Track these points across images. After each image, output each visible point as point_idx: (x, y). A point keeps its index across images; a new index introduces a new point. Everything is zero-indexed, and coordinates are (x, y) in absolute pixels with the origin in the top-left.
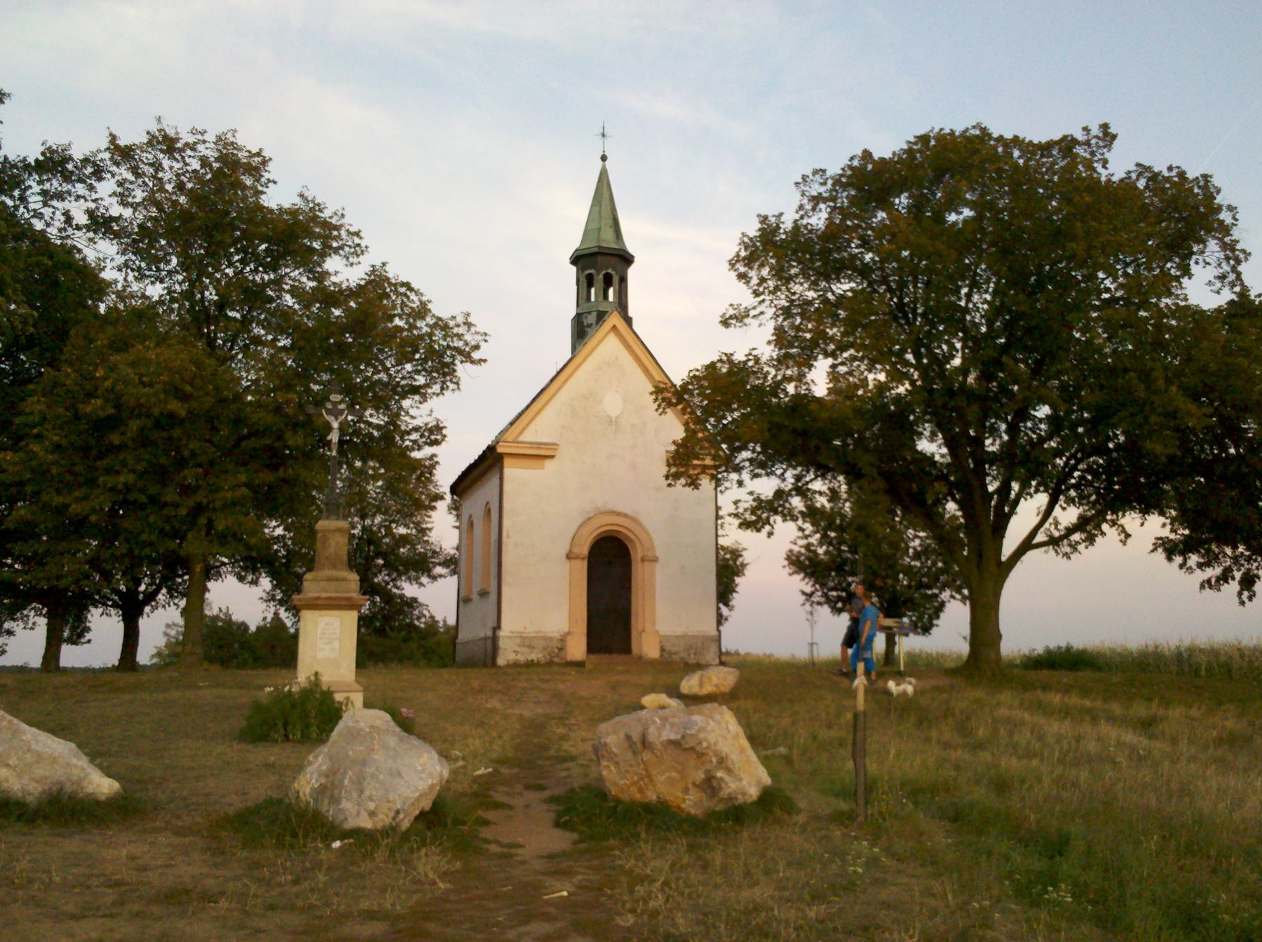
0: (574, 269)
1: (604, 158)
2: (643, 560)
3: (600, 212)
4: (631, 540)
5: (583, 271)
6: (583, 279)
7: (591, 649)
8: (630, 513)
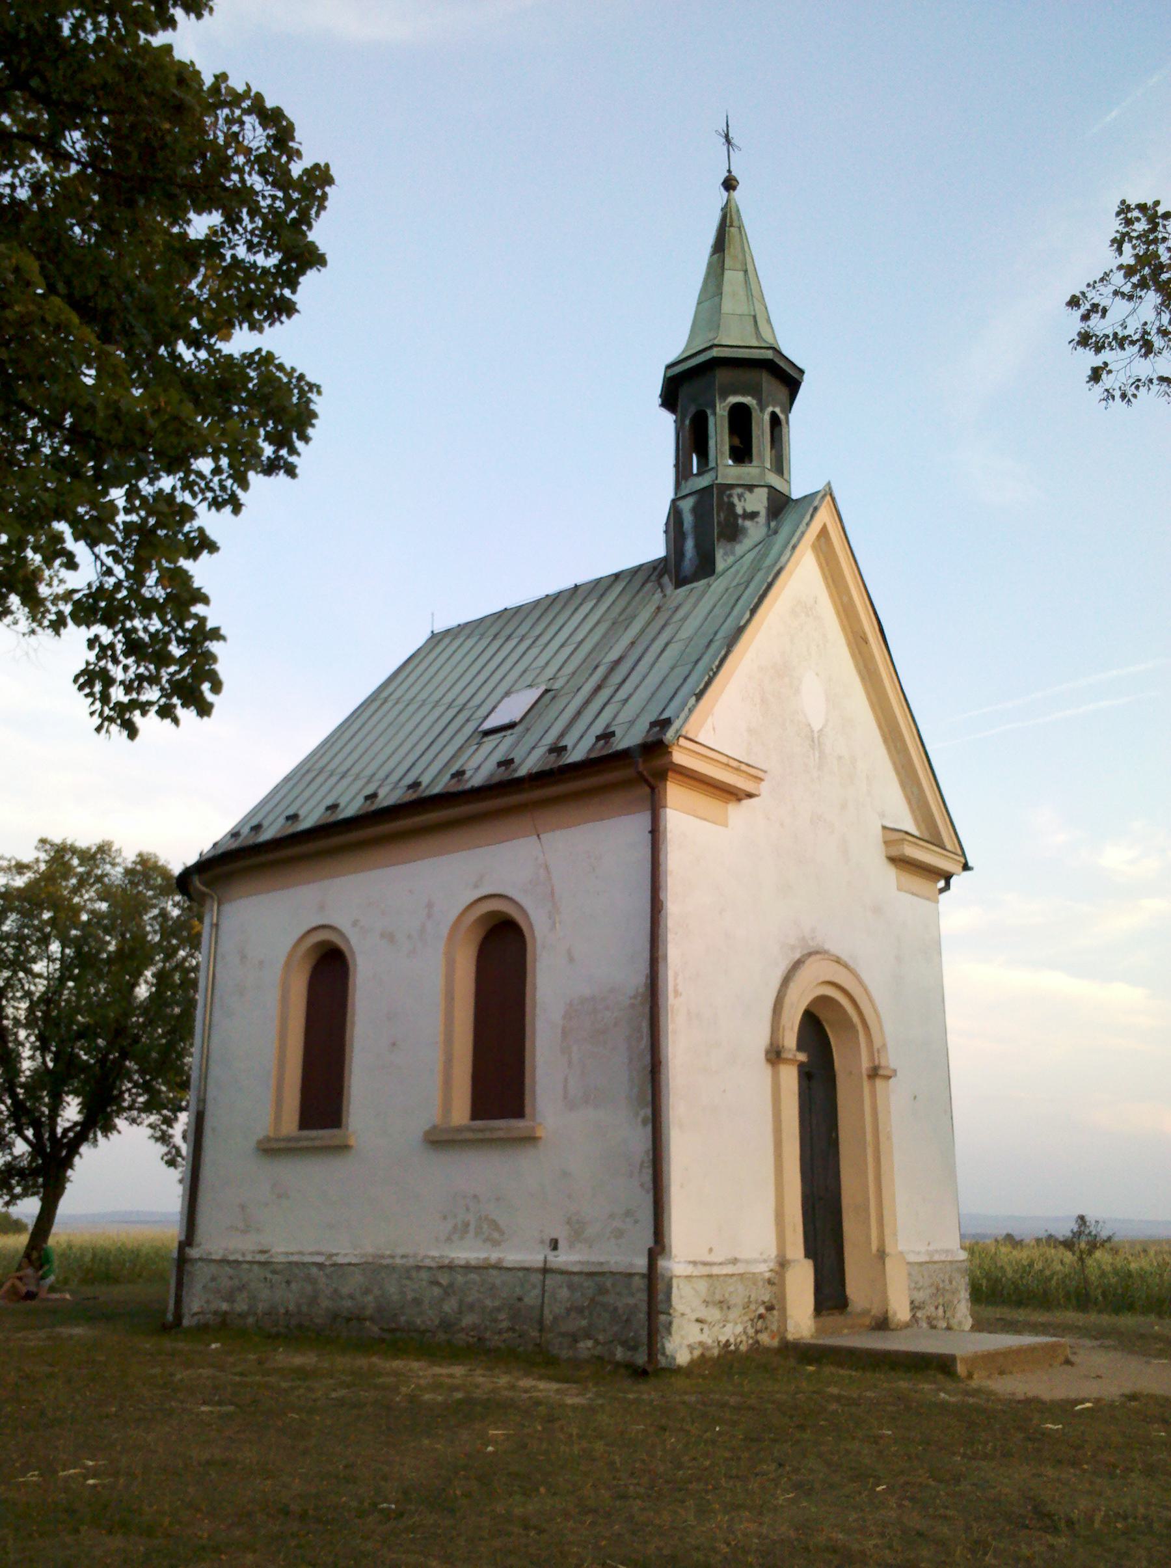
1: (729, 184)
4: (849, 1025)
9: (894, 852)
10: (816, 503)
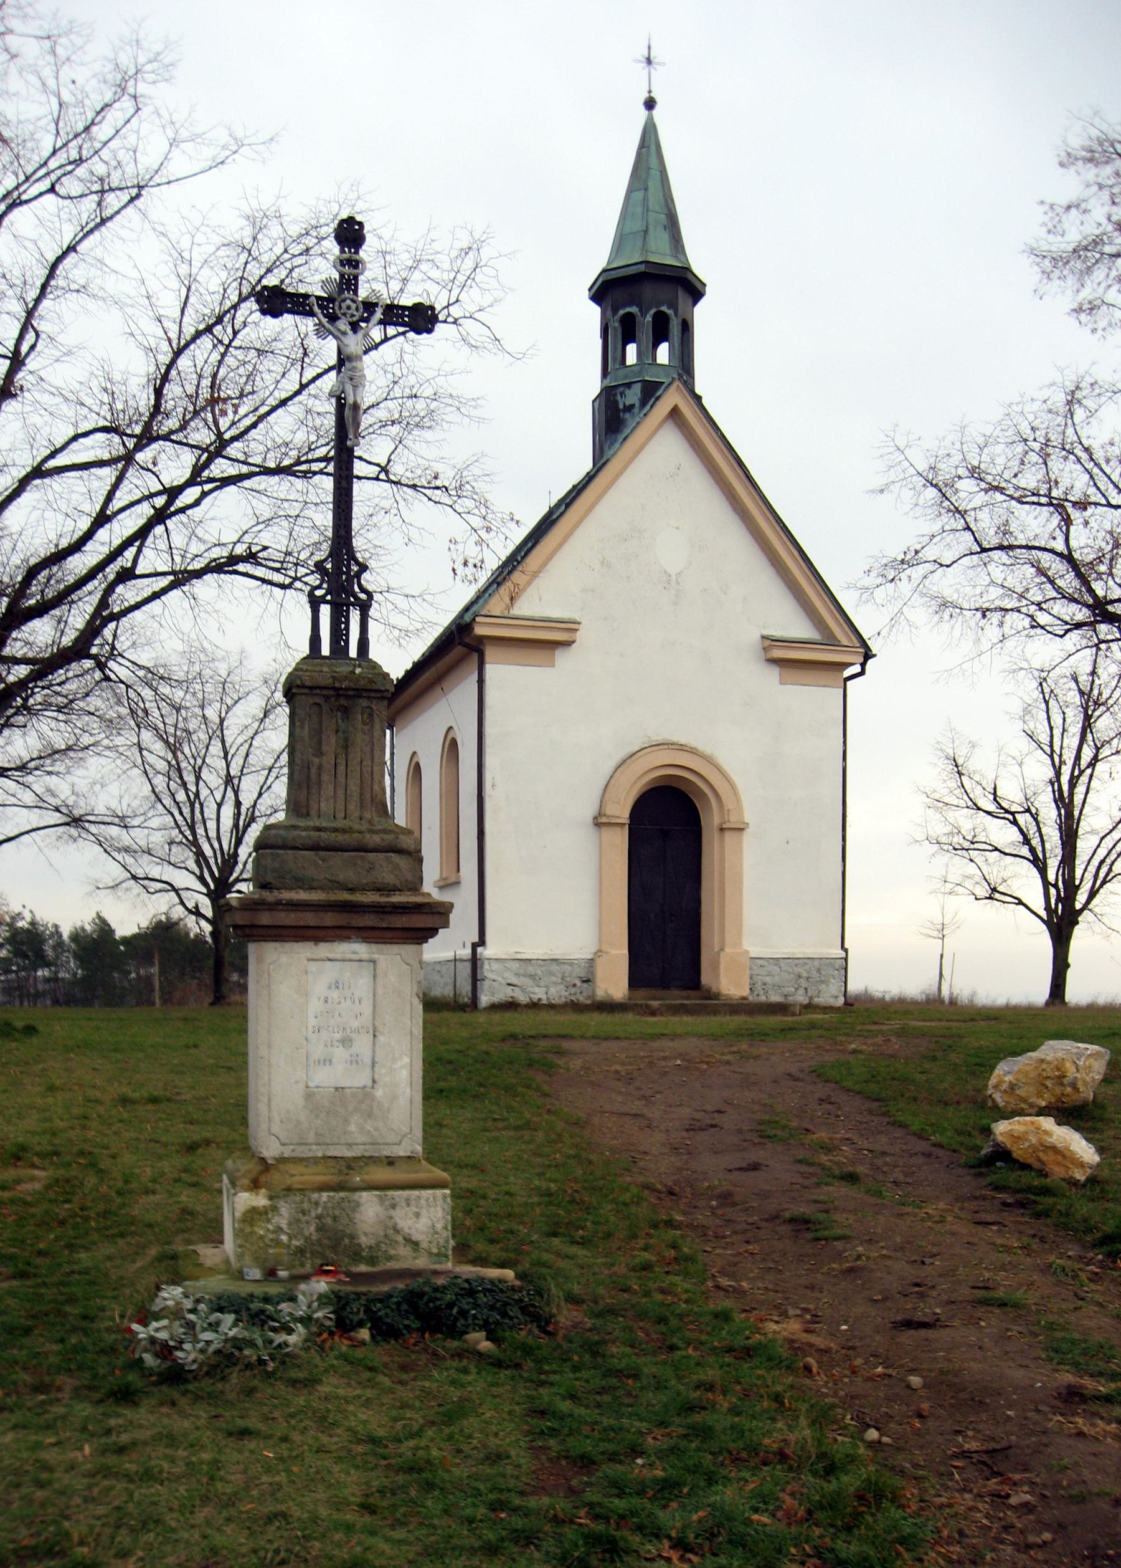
0: (595, 311)
1: (650, 104)
2: (722, 830)
3: (645, 200)
5: (615, 311)
6: (615, 324)
7: (636, 980)
8: (701, 747)
9: (769, 656)
10: (658, 393)
